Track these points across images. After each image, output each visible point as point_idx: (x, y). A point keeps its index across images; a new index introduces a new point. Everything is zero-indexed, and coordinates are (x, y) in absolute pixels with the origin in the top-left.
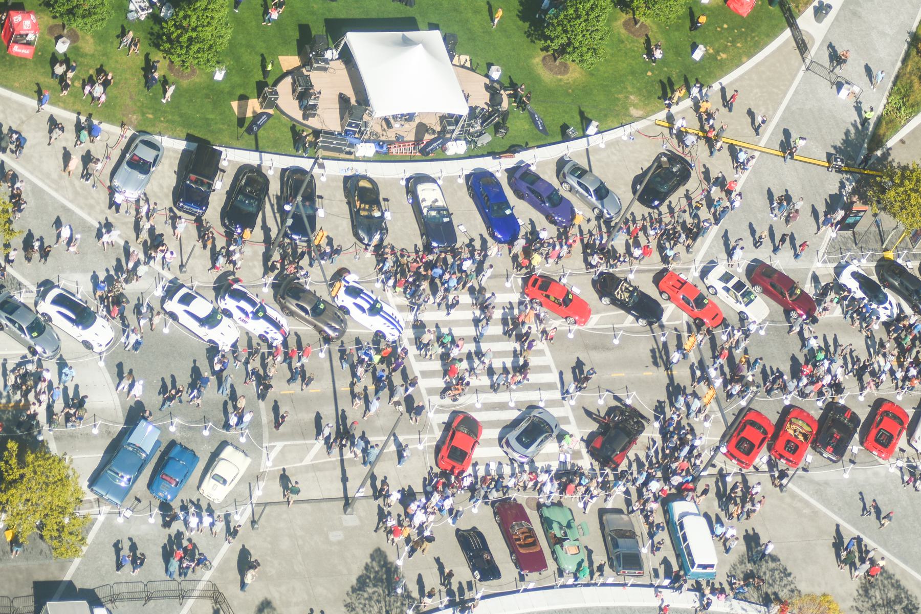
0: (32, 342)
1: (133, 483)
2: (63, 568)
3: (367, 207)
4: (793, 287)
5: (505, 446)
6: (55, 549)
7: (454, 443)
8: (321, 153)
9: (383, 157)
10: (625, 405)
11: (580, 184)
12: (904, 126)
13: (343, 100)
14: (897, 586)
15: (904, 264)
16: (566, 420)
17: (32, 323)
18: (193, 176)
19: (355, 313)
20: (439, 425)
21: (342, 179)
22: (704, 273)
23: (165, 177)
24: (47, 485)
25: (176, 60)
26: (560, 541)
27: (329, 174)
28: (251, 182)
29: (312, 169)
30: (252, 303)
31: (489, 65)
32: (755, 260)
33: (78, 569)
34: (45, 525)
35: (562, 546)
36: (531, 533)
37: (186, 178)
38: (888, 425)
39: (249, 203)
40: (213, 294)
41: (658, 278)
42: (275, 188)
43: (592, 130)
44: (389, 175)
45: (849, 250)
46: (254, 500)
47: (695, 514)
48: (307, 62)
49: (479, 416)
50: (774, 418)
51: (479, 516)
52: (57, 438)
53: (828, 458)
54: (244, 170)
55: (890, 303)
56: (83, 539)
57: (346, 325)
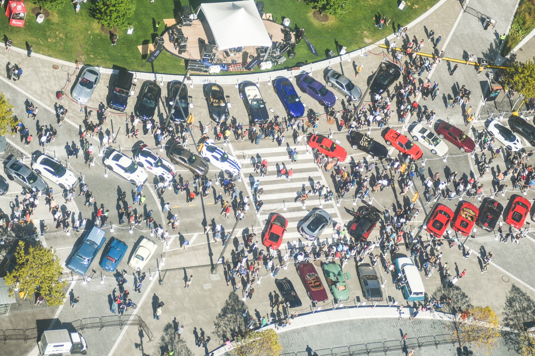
0: (30, 186)
1: (91, 262)
2: (53, 312)
3: (217, 101)
4: (461, 134)
5: (301, 231)
6: (48, 301)
8: (190, 72)
9: (225, 73)
10: (368, 205)
11: (337, 82)
12: (521, 40)
13: (201, 42)
14: (528, 300)
15: (524, 118)
16: (335, 215)
17: (30, 175)
18: (118, 89)
19: (213, 161)
20: (263, 221)
21: (202, 86)
22: (411, 129)
23: (102, 90)
24: (42, 265)
25: (105, 23)
26: (335, 283)
27: (195, 83)
28: (151, 91)
29: (184, 80)
30: (154, 158)
31: (283, 18)
32: (439, 120)
33: (62, 312)
34: (42, 288)
35: (336, 286)
36: (318, 279)
37: (113, 90)
38: (519, 209)
39: (150, 102)
40: (132, 154)
41: (384, 133)
42: (164, 93)
43: (343, 51)
44: (229, 83)
45: (493, 112)
46: (160, 268)
47: (411, 265)
48: (179, 22)
49: (286, 215)
50: (453, 208)
51: (289, 271)
52: (47, 239)
53: (486, 230)
54: (146, 83)
55: (518, 141)
56: (63, 294)
57: (208, 168)
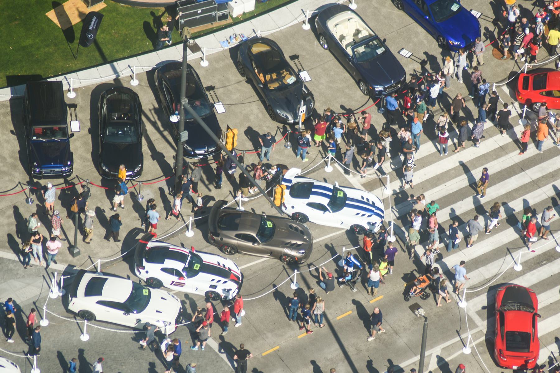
3: (274, 76)
7: (510, 327)
8: (188, 32)
18: (37, 128)
19: (314, 216)
20: (478, 313)
21: (228, 53)
27: (209, 52)
29: (185, 56)
30: (180, 257)
37: (29, 134)
39: (124, 133)
40: (126, 266)
42: (148, 101)
49: (525, 281)
54: (99, 93)
57: (309, 235)
